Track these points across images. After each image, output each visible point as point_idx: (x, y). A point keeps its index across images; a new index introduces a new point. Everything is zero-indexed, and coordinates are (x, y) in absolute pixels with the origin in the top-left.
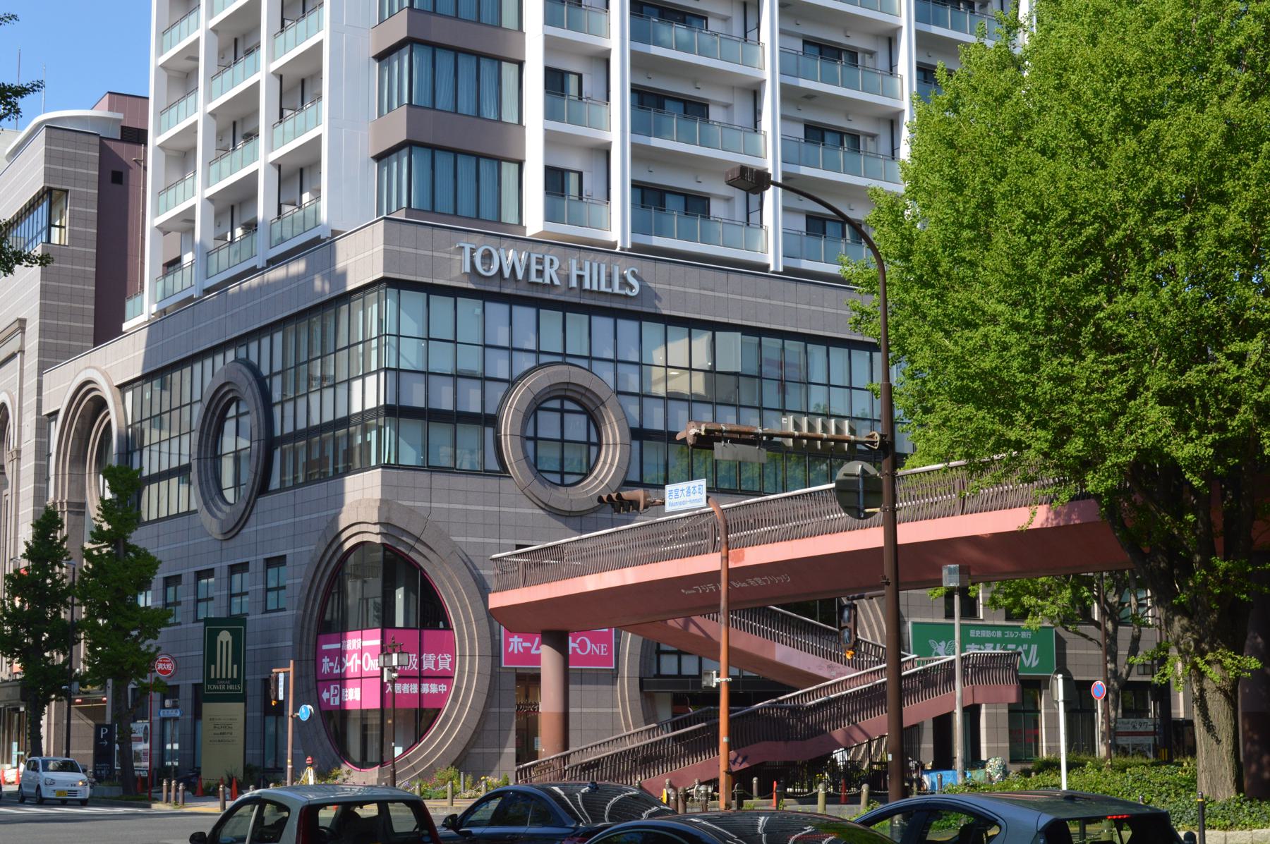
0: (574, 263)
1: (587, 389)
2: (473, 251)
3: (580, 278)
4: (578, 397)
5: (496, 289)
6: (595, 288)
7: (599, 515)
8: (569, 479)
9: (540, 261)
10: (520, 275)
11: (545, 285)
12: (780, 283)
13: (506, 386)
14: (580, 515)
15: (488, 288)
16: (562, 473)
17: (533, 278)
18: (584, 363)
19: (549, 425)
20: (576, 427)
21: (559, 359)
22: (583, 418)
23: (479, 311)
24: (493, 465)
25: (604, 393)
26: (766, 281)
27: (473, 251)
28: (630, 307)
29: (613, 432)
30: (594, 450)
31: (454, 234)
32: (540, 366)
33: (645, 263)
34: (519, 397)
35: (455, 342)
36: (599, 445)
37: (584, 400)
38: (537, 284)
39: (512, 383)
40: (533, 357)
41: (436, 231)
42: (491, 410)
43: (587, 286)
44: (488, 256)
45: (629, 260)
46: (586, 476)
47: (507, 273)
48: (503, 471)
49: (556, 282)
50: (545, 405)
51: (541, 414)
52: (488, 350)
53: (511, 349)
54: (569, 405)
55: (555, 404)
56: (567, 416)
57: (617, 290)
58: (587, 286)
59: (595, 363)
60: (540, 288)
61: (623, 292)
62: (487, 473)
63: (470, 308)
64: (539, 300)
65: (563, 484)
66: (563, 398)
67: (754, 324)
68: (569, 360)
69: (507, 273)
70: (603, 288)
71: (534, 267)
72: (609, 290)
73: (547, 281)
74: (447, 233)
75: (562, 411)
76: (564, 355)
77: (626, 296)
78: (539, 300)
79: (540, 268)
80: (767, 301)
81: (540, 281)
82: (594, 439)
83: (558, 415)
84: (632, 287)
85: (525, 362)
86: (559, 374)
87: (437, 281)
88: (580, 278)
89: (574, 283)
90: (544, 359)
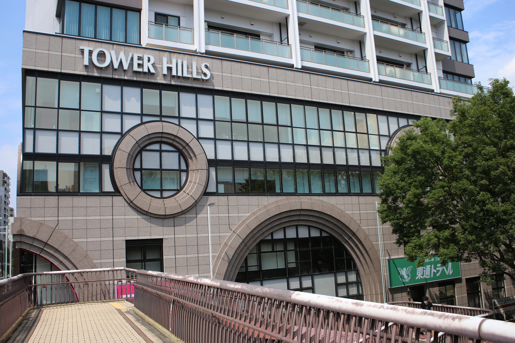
0: (165, 60)
1: (176, 136)
2: (91, 52)
3: (170, 69)
4: (171, 142)
5: (110, 76)
6: (180, 74)
7: (187, 216)
8: (166, 194)
9: (139, 58)
10: (126, 67)
11: (145, 73)
12: (301, 74)
13: (119, 137)
14: (173, 216)
15: (104, 75)
16: (162, 191)
17: (136, 68)
18: (176, 121)
19: (150, 160)
20: (171, 161)
21: (158, 119)
22: (176, 155)
23: (98, 90)
24: (108, 187)
25: (187, 138)
26: (292, 72)
27: (91, 52)
28: (205, 87)
29: (198, 165)
30: (184, 176)
31: (78, 41)
32: (142, 123)
33: (215, 61)
34: (128, 144)
35: (80, 110)
36: (187, 171)
37: (175, 143)
38: (139, 73)
39: (122, 135)
40: (139, 118)
41: (65, 40)
42: (108, 152)
43: (174, 73)
44: (102, 55)
45: (204, 59)
46: (178, 191)
47: (116, 66)
48: (117, 192)
49: (152, 71)
50: (148, 148)
51: (144, 154)
52: (104, 115)
53: (122, 114)
54: (165, 147)
55: (156, 147)
56: (164, 154)
57: (195, 76)
58: (174, 73)
59: (182, 121)
60: (142, 75)
61: (199, 77)
62: (102, 194)
63: (91, 90)
64: (143, 83)
65: (162, 197)
66: (161, 143)
67: (286, 96)
68: (163, 119)
69: (116, 66)
70: (185, 75)
71: (136, 62)
72: (190, 76)
73: (146, 70)
74: (74, 41)
75: (161, 151)
76: (161, 116)
77: (203, 80)
78: (143, 83)
79: (141, 62)
80: (294, 84)
81: (140, 70)
82: (183, 167)
83: (158, 154)
84: (205, 75)
85: (130, 122)
86: (156, 127)
87: (63, 71)
88: (170, 69)
89: (165, 72)
90: (145, 119)
